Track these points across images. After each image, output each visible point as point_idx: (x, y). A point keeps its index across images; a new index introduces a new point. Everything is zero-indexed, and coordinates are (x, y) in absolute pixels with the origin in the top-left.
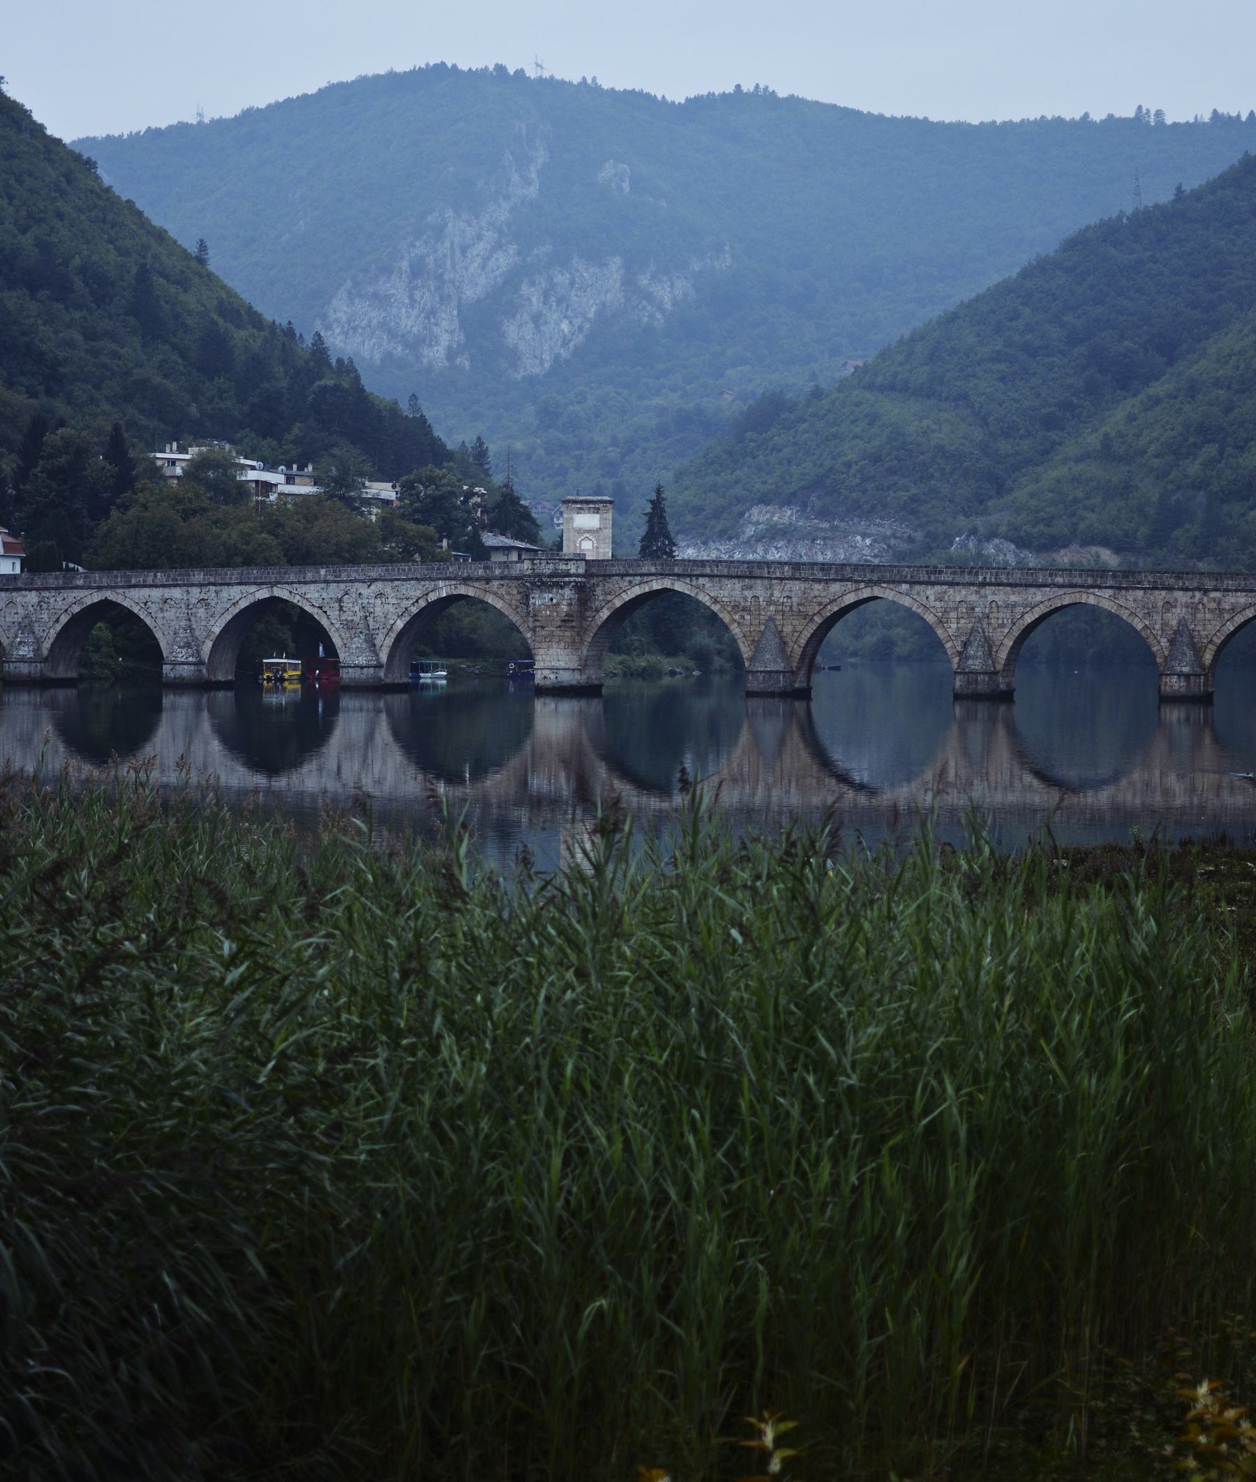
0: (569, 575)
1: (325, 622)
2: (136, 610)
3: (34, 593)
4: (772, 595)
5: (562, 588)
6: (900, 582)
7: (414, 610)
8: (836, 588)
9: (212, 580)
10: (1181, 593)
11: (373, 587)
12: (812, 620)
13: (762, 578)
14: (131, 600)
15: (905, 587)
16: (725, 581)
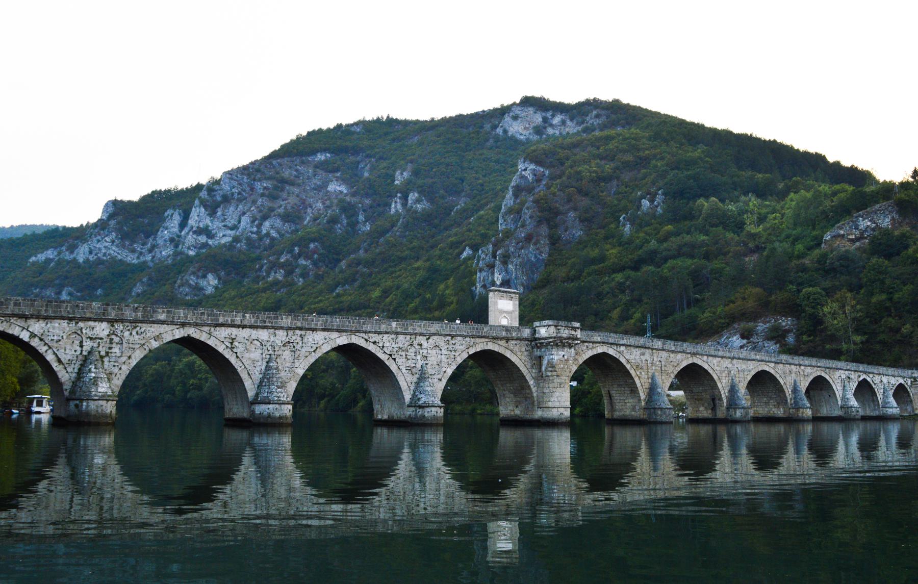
0: (577, 339)
1: (393, 367)
2: (221, 349)
3: (104, 325)
4: (653, 360)
5: (570, 346)
6: (704, 355)
7: (459, 360)
8: (679, 356)
9: (299, 324)
10: (793, 367)
11: (430, 340)
12: (670, 376)
13: (649, 348)
14: (217, 339)
15: (705, 357)
16: (632, 348)
